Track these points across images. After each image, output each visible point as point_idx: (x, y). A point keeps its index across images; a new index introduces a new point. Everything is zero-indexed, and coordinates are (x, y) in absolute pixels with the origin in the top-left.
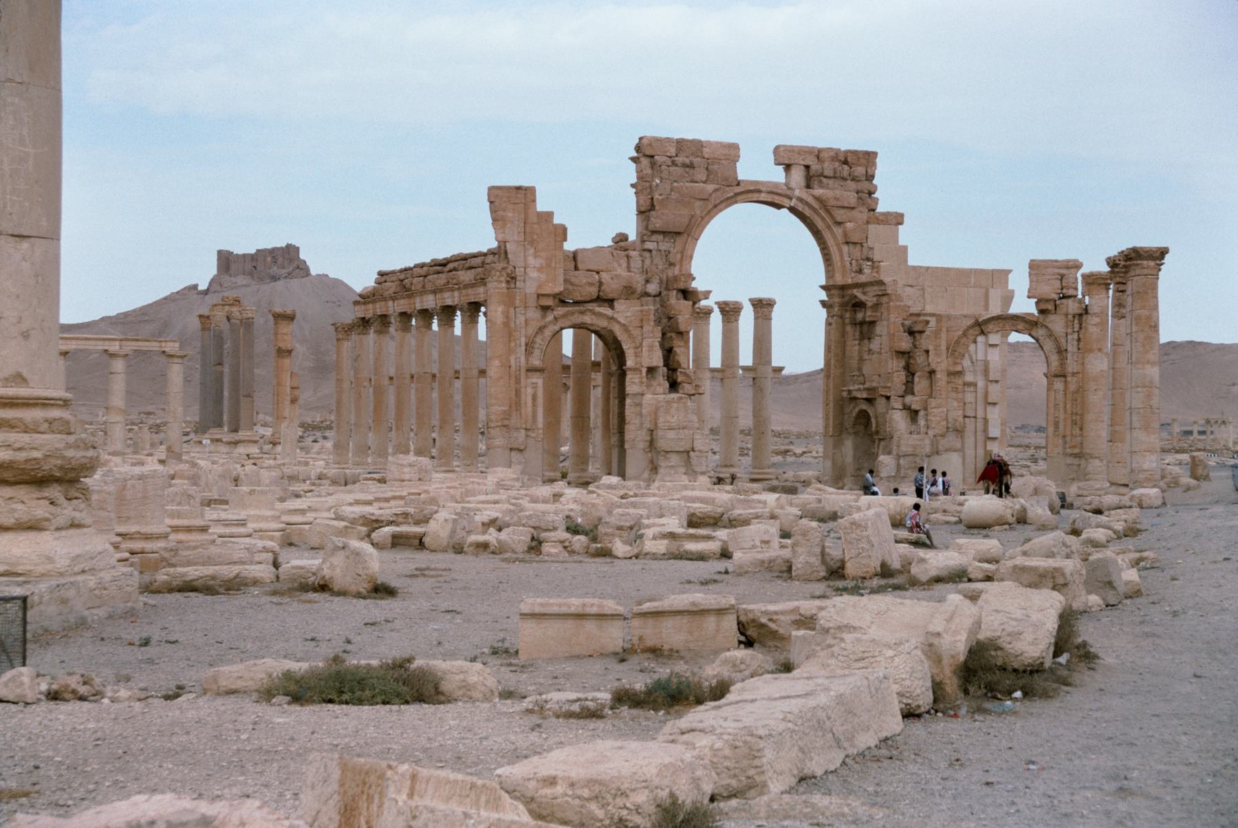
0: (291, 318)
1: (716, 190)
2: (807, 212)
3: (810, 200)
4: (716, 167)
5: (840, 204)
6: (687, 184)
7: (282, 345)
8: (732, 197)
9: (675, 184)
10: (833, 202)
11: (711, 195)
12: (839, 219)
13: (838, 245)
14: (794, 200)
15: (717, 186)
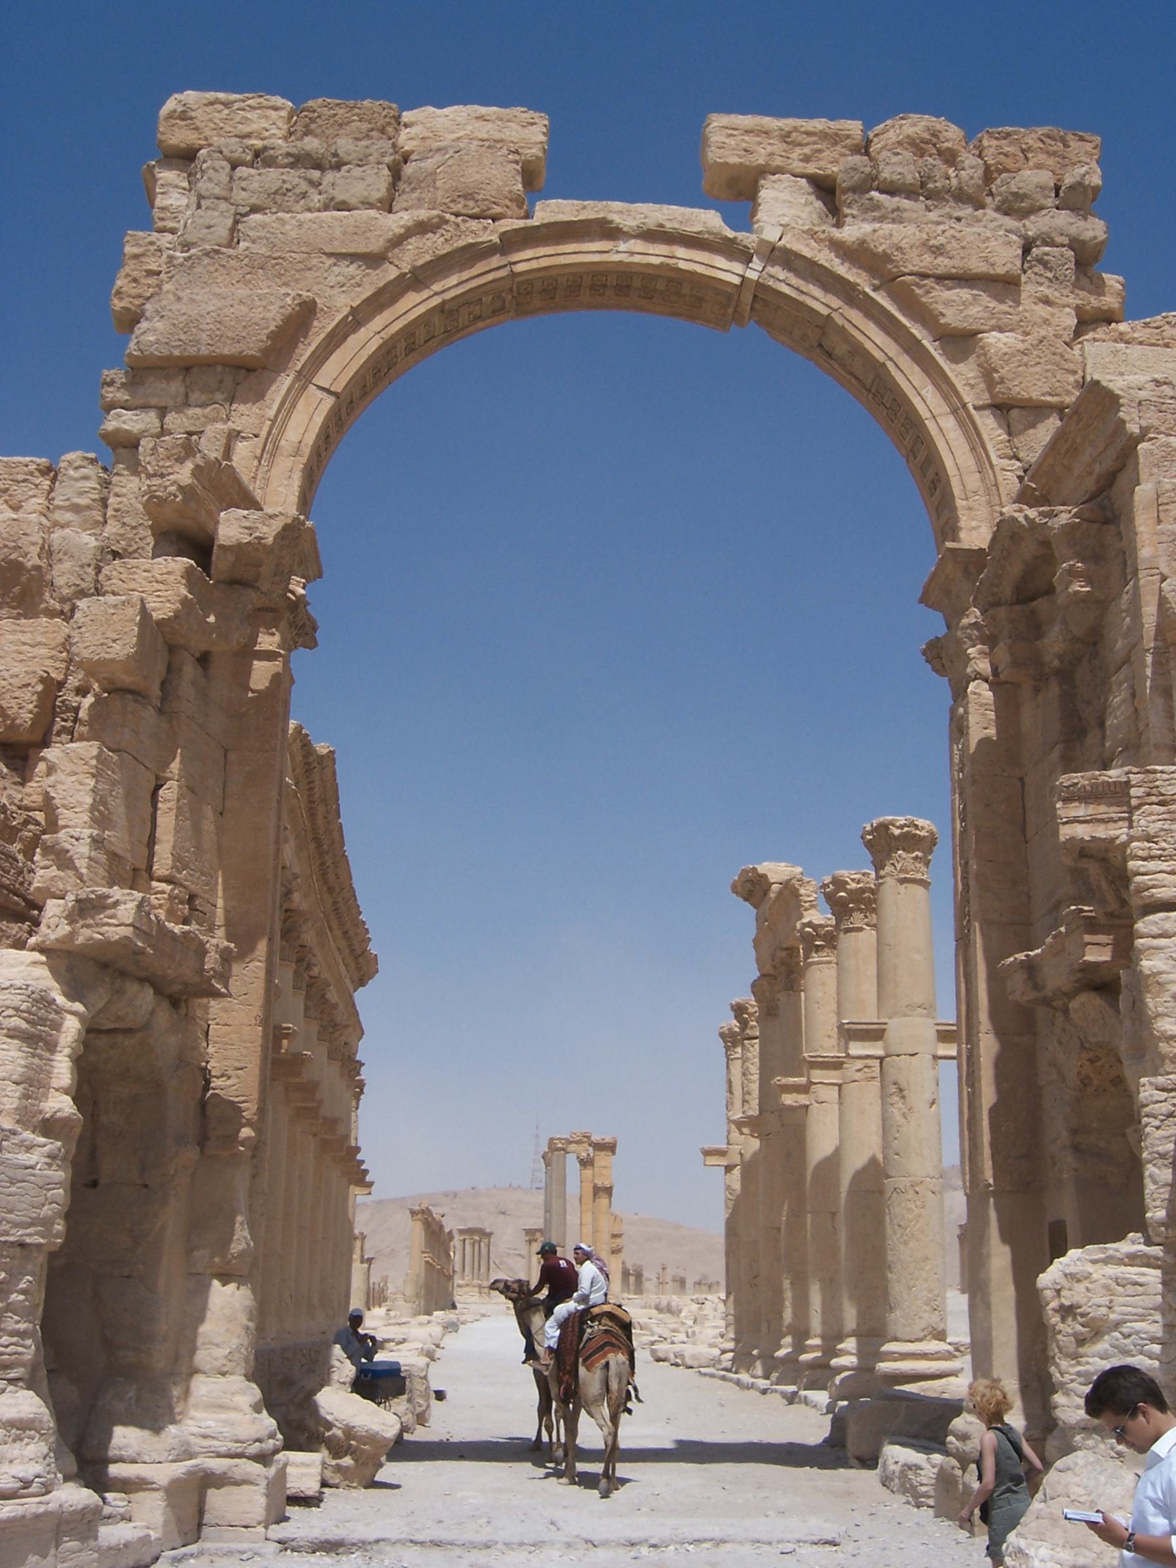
0: (611, 1148)
1: (422, 228)
2: (819, 300)
3: (826, 258)
4: (429, 164)
5: (943, 264)
6: (309, 215)
7: (599, 1183)
8: (490, 250)
9: (256, 217)
10: (926, 262)
11: (398, 241)
12: (952, 318)
13: (958, 409)
14: (756, 264)
15: (423, 214)
